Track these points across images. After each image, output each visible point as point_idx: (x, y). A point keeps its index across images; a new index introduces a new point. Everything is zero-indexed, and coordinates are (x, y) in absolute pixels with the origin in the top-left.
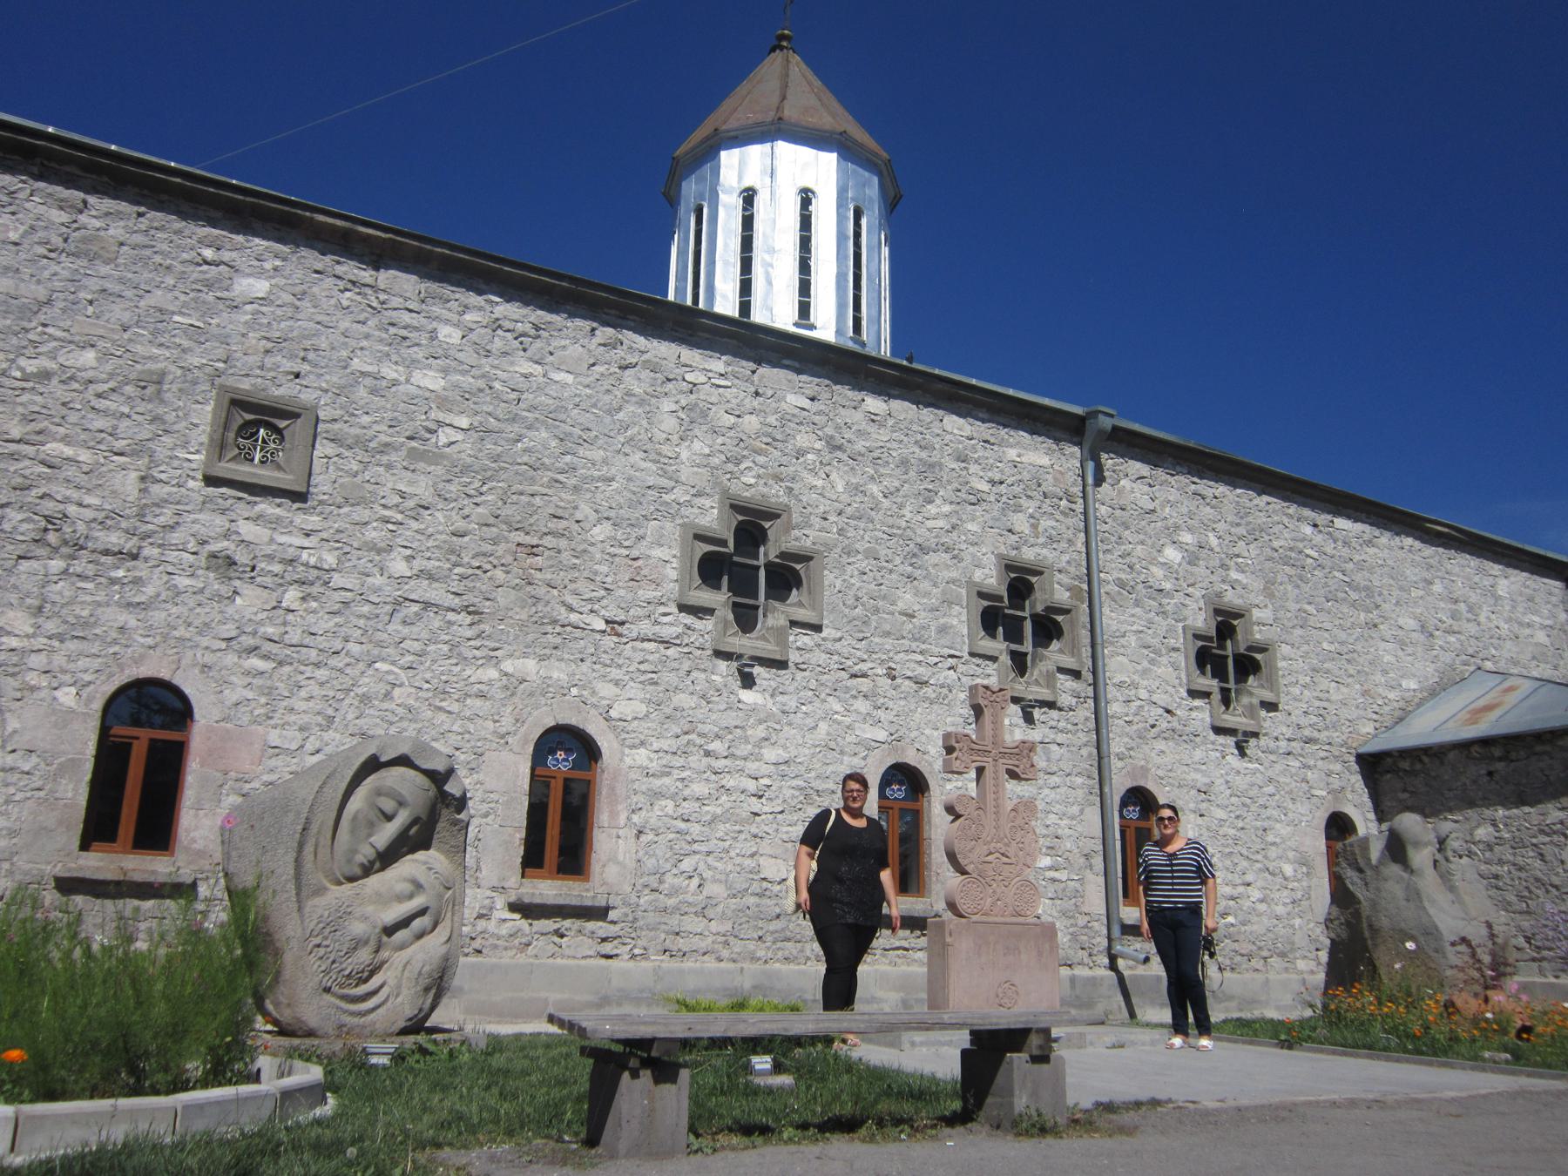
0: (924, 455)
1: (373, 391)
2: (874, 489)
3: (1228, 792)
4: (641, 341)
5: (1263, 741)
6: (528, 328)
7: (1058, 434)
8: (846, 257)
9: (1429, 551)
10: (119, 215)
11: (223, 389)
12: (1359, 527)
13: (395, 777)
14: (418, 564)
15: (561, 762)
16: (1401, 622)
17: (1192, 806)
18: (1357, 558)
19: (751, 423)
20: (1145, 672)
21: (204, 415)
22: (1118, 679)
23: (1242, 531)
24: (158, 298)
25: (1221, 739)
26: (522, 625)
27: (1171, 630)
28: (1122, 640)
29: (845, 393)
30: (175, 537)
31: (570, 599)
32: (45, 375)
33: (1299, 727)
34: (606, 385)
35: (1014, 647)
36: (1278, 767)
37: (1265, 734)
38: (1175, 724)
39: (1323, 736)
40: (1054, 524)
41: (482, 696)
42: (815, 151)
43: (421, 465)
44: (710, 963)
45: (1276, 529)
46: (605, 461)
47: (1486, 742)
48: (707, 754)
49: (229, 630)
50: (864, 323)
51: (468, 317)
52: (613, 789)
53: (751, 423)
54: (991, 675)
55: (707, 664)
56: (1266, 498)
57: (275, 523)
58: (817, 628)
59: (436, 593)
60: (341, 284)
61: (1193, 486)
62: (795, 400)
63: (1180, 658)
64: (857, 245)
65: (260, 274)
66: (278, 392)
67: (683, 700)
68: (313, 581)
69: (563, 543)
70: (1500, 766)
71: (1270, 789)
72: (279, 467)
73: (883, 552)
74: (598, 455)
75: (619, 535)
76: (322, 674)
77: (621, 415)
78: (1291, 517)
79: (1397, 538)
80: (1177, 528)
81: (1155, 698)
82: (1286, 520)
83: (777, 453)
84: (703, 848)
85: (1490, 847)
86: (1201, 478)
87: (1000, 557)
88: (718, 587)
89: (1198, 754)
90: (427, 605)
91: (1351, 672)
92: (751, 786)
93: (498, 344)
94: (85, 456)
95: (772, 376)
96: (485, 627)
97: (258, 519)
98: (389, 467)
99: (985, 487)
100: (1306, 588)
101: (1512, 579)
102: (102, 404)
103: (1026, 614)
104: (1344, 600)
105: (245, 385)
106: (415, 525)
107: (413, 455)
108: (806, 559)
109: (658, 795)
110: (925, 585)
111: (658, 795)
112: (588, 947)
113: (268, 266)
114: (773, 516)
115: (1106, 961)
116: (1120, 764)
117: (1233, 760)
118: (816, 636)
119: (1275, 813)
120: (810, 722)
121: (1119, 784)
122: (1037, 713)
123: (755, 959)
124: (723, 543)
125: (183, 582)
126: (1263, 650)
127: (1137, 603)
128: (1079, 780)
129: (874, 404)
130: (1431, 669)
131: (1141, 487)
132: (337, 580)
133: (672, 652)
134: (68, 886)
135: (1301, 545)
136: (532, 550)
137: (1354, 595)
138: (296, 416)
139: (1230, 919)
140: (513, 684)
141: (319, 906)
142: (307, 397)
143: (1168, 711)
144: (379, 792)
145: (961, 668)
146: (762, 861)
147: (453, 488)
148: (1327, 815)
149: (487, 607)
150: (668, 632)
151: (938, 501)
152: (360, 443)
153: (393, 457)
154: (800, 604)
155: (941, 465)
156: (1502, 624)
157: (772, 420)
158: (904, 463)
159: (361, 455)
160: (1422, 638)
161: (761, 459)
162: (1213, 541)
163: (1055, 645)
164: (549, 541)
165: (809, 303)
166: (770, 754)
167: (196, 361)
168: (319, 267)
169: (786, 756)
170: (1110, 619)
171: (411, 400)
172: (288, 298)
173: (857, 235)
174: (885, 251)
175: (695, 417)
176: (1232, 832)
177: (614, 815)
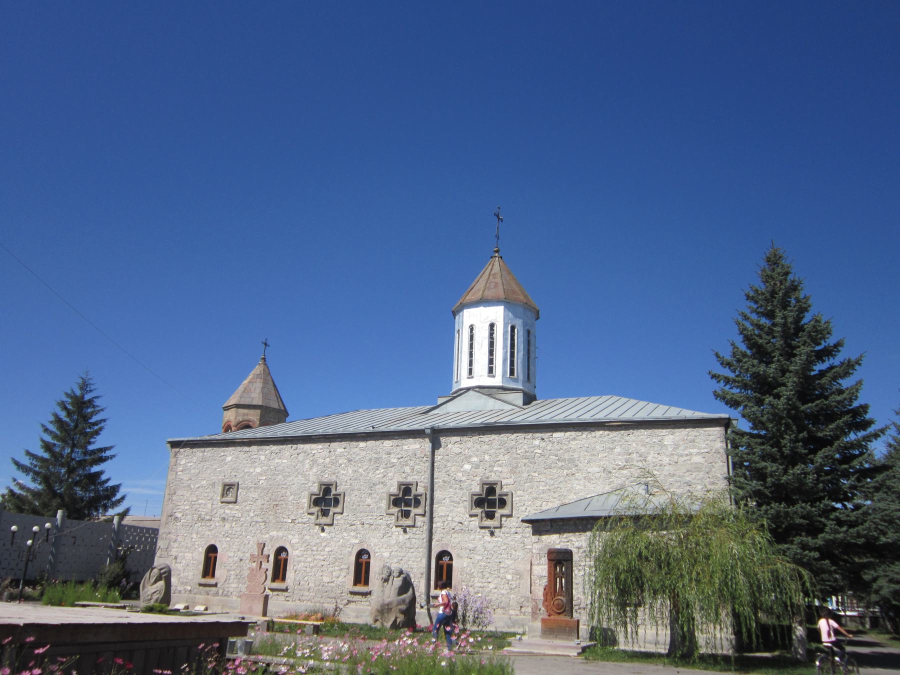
2: (360, 470)
3: (483, 550)
4: (301, 446)
5: (503, 529)
10: (210, 451)
12: (568, 434)
14: (255, 513)
16: (589, 470)
17: (466, 555)
18: (565, 447)
20: (451, 511)
21: (219, 489)
24: (215, 466)
25: (483, 531)
26: (274, 523)
28: (444, 501)
29: (354, 443)
30: (216, 515)
31: (284, 516)
32: (199, 487)
34: (294, 460)
36: (510, 539)
37: (505, 527)
40: (419, 467)
43: (257, 490)
44: (309, 603)
45: (519, 446)
46: (293, 480)
49: (223, 533)
55: (312, 527)
56: (515, 435)
57: (231, 509)
59: (259, 519)
61: (480, 439)
62: (339, 450)
63: (466, 503)
65: (230, 455)
66: (232, 481)
67: (307, 537)
68: (236, 520)
69: (283, 502)
71: (504, 547)
74: (291, 479)
76: (238, 540)
77: (297, 467)
79: (593, 433)
80: (471, 456)
84: (310, 574)
86: (484, 435)
89: (472, 537)
90: (257, 522)
91: (556, 496)
92: (322, 558)
97: (229, 509)
98: (251, 492)
99: (395, 460)
101: (677, 434)
102: (207, 490)
103: (412, 497)
104: (555, 467)
106: (255, 504)
107: (255, 488)
109: (300, 561)
110: (375, 495)
111: (300, 561)
112: (283, 598)
114: (332, 485)
116: (437, 543)
117: (488, 537)
118: (341, 516)
119: (505, 556)
120: (338, 540)
122: (408, 529)
124: (319, 495)
125: (217, 524)
126: (507, 495)
127: (450, 487)
128: (421, 550)
129: (362, 444)
132: (242, 519)
133: (305, 526)
134: (200, 585)
135: (532, 450)
137: (560, 464)
138: (234, 485)
139: (480, 595)
140: (272, 538)
141: (146, 590)
142: (237, 480)
143: (461, 523)
151: (380, 469)
152: (246, 488)
153: (252, 489)
155: (381, 458)
157: (333, 458)
158: (370, 460)
160: (603, 475)
161: (330, 469)
162: (487, 457)
164: (280, 503)
165: (493, 359)
166: (327, 549)
172: (234, 459)
175: (314, 462)
176: (483, 564)
177: (290, 567)
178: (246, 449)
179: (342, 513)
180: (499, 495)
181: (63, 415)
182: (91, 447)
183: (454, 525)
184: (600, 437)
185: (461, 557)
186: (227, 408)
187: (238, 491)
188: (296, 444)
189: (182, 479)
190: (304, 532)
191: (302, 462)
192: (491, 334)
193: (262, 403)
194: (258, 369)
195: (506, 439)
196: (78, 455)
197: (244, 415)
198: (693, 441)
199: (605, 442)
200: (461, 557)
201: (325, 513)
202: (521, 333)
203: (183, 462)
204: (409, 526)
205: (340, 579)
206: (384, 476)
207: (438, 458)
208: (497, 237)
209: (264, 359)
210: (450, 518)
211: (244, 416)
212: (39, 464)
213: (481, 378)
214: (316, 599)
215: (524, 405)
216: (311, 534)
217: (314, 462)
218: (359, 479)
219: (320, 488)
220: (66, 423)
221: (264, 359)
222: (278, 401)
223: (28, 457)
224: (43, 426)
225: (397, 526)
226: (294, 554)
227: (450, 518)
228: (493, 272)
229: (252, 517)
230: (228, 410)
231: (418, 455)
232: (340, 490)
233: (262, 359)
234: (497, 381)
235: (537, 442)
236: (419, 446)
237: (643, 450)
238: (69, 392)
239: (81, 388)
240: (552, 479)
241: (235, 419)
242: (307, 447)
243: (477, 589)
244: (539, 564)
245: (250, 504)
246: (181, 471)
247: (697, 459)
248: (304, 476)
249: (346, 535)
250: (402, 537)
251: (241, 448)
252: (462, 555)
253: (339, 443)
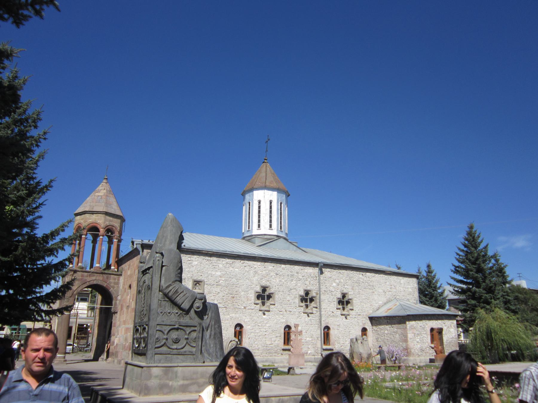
0: (291, 273)
1: (211, 276)
2: (283, 280)
4: (247, 262)
6: (231, 263)
7: (314, 266)
8: (279, 214)
9: (386, 276)
11: (193, 279)
13: (233, 342)
15: (238, 329)
16: (379, 291)
18: (371, 280)
19: (264, 272)
20: (329, 306)
22: (324, 307)
23: (348, 278)
25: (342, 316)
27: (334, 298)
28: (325, 301)
31: (239, 304)
33: (357, 313)
34: (243, 270)
35: (306, 303)
36: (353, 320)
38: (334, 314)
39: (362, 314)
40: (313, 282)
41: (227, 320)
42: (272, 192)
43: (218, 287)
45: (354, 277)
46: (243, 282)
47: (387, 317)
48: (258, 326)
50: (282, 227)
51: (223, 262)
52: (245, 332)
53: (264, 272)
54: (302, 309)
56: (352, 272)
60: (206, 260)
62: (271, 268)
64: (281, 210)
65: (196, 261)
67: (255, 318)
69: (237, 296)
70: (389, 321)
71: (351, 324)
72: (200, 290)
73: (285, 291)
75: (245, 293)
77: (245, 275)
78: (358, 274)
80: (335, 279)
81: (330, 310)
82: (357, 275)
83: (268, 277)
85: (387, 334)
87: (304, 289)
88: (259, 300)
89: (338, 319)
92: (265, 330)
93: (227, 266)
95: (267, 264)
96: (228, 310)
98: (214, 287)
99: (301, 277)
100: (360, 287)
106: (218, 296)
107: (217, 285)
108: (272, 294)
110: (291, 295)
111: (252, 333)
113: (197, 259)
114: (268, 287)
115: (321, 355)
120: (273, 320)
121: (323, 325)
122: (310, 315)
123: (266, 356)
126: (351, 300)
127: (328, 294)
128: (316, 325)
129: (283, 266)
130: (385, 299)
131: (329, 273)
135: (359, 279)
136: (233, 297)
137: (370, 287)
138: (202, 282)
139: (343, 347)
140: (231, 318)
142: (203, 279)
144: (232, 344)
145: (297, 309)
146: (267, 342)
147: (222, 289)
148: (362, 328)
149: (227, 307)
150: (252, 308)
152: (210, 284)
154: (272, 301)
155: (294, 275)
156: (401, 289)
157: (267, 271)
158: (288, 275)
159: (210, 286)
160: (383, 293)
161: (266, 278)
162: (342, 281)
163: (313, 303)
164: (235, 296)
166: (267, 325)
167: (189, 276)
168: (203, 258)
169: (270, 325)
170: (322, 297)
171: (216, 277)
172: (200, 264)
173: (281, 208)
174: (287, 209)
175: (256, 272)
177: (246, 336)
178: (207, 258)
180: (348, 300)
183: (330, 313)
185: (334, 329)
190: (253, 315)
197: (110, 220)
198: (409, 283)
200: (334, 329)
205: (276, 342)
206: (296, 285)
207: (322, 278)
209: (107, 179)
210: (328, 310)
211: (110, 222)
214: (263, 354)
216: (257, 316)
217: (256, 272)
218: (283, 286)
225: (304, 313)
226: (247, 328)
227: (328, 310)
230: (93, 214)
233: (107, 179)
237: (395, 284)
240: (367, 294)
241: (104, 223)
243: (341, 344)
244: (410, 333)
245: (214, 296)
247: (410, 290)
249: (277, 317)
250: (307, 319)
251: (204, 257)
252: (334, 328)
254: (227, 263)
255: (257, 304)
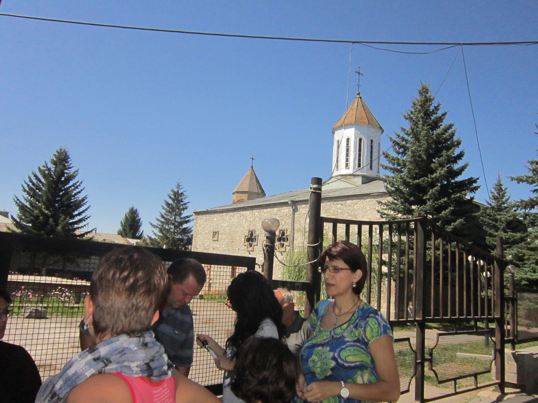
4: (241, 212)
12: (354, 201)
18: (352, 208)
21: (212, 234)
28: (298, 239)
29: (262, 210)
45: (331, 209)
46: (239, 229)
56: (329, 203)
58: (257, 245)
65: (216, 218)
74: (237, 229)
79: (366, 200)
90: (225, 250)
94: (206, 240)
105: (214, 230)
122: (283, 253)
124: (248, 236)
129: (265, 210)
132: (220, 248)
135: (337, 210)
136: (233, 242)
150: (243, 249)
153: (224, 234)
157: (254, 218)
164: (234, 240)
179: (257, 245)
181: (171, 202)
182: (183, 216)
184: (369, 202)
186: (234, 194)
187: (218, 234)
188: (240, 211)
189: (198, 230)
191: (242, 220)
192: (348, 145)
193: (249, 190)
194: (249, 172)
195: (325, 205)
196: (178, 219)
199: (371, 205)
201: (251, 245)
202: (366, 142)
203: (199, 222)
204: (283, 252)
207: (296, 216)
208: (359, 86)
212: (161, 224)
213: (343, 171)
215: (362, 183)
219: (249, 233)
220: (171, 205)
221: (252, 167)
222: (258, 189)
223: (157, 221)
224: (162, 206)
228: (353, 107)
229: (224, 248)
231: (288, 215)
232: (257, 233)
234: (350, 171)
235: (339, 206)
236: (288, 210)
238: (171, 189)
239: (177, 188)
241: (236, 198)
242: (244, 212)
246: (199, 226)
248: (243, 227)
253: (256, 210)
254: (231, 216)
255: (245, 246)
